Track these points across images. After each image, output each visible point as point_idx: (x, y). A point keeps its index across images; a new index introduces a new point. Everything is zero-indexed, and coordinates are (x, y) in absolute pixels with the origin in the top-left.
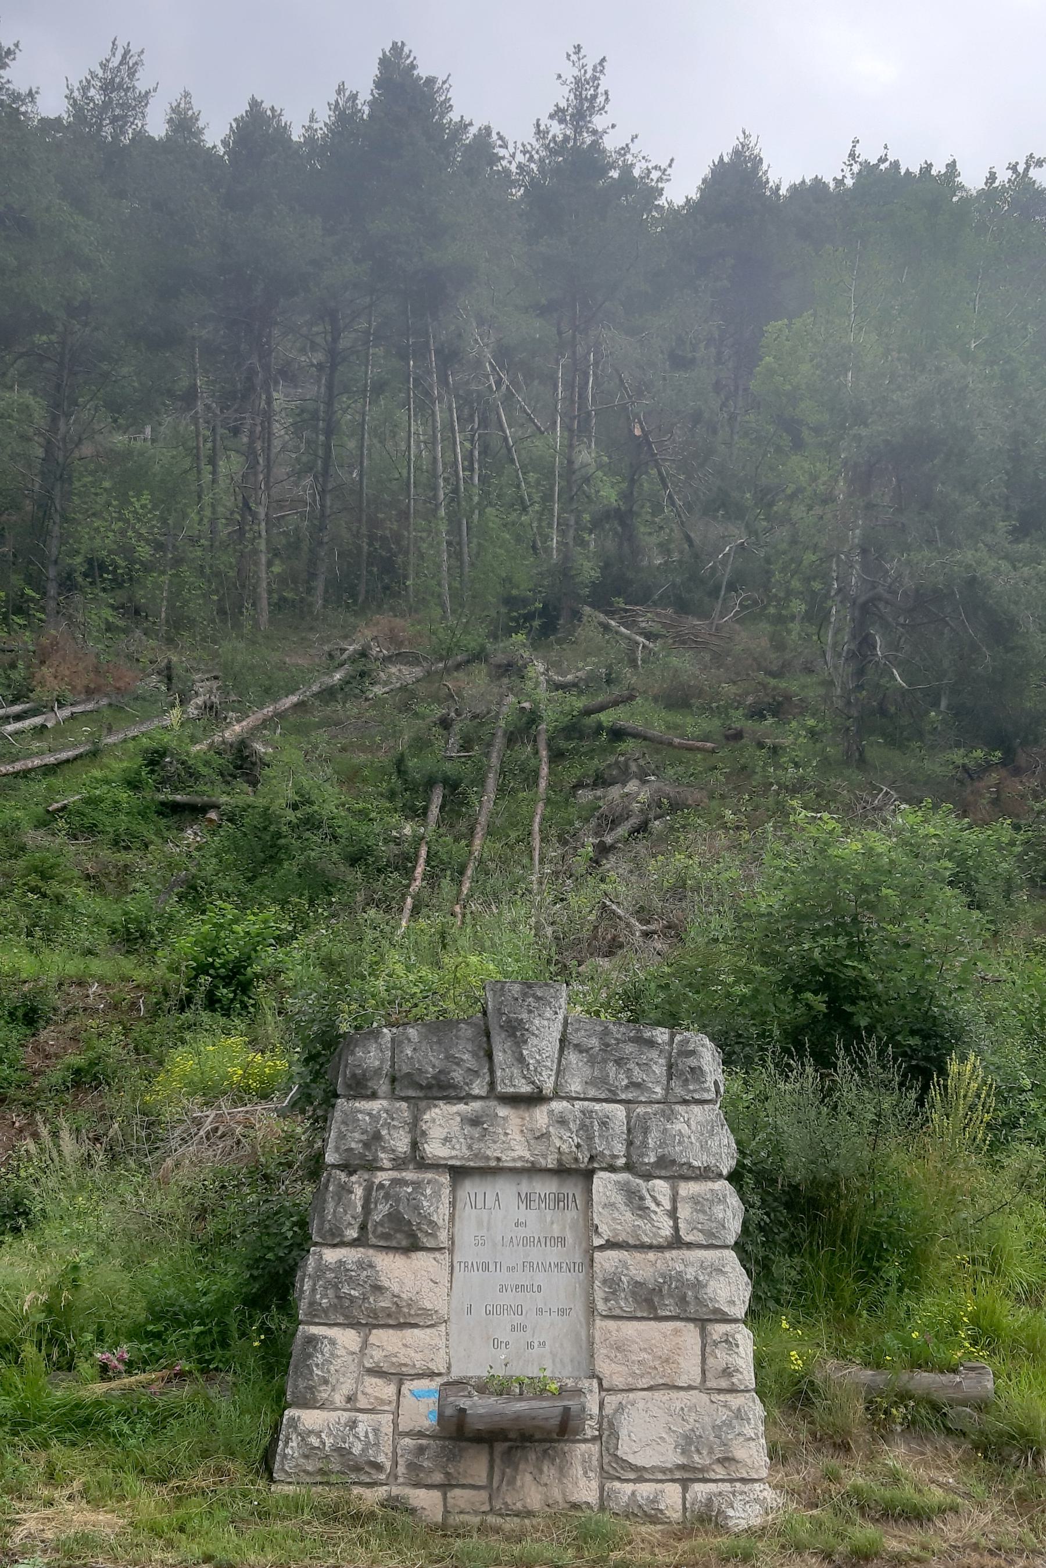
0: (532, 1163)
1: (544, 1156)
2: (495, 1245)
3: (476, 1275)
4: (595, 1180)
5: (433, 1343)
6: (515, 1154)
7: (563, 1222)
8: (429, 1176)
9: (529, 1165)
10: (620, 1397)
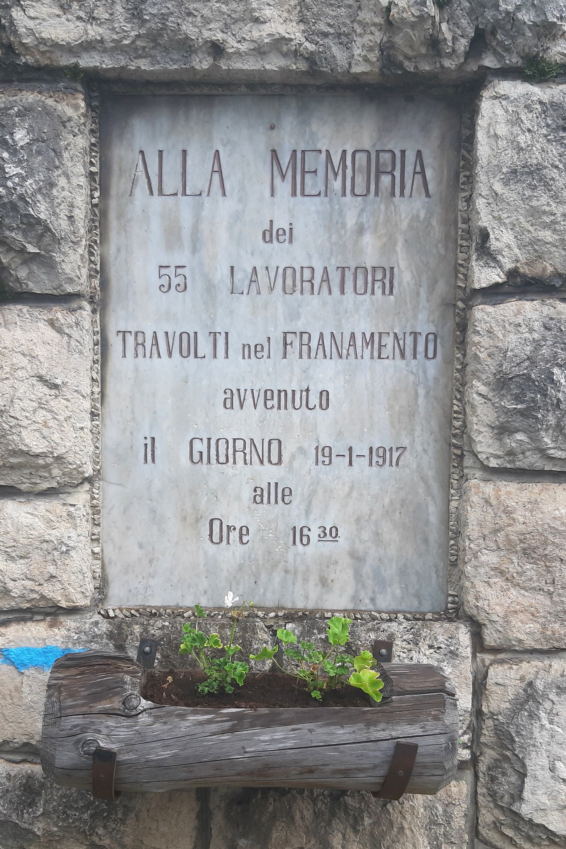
0: (311, 59)
1: (344, 39)
2: (210, 288)
3: (165, 369)
4: (487, 106)
5: (53, 535)
6: (262, 33)
7: (391, 229)
8: (30, 97)
9: (302, 66)
10: (529, 668)
